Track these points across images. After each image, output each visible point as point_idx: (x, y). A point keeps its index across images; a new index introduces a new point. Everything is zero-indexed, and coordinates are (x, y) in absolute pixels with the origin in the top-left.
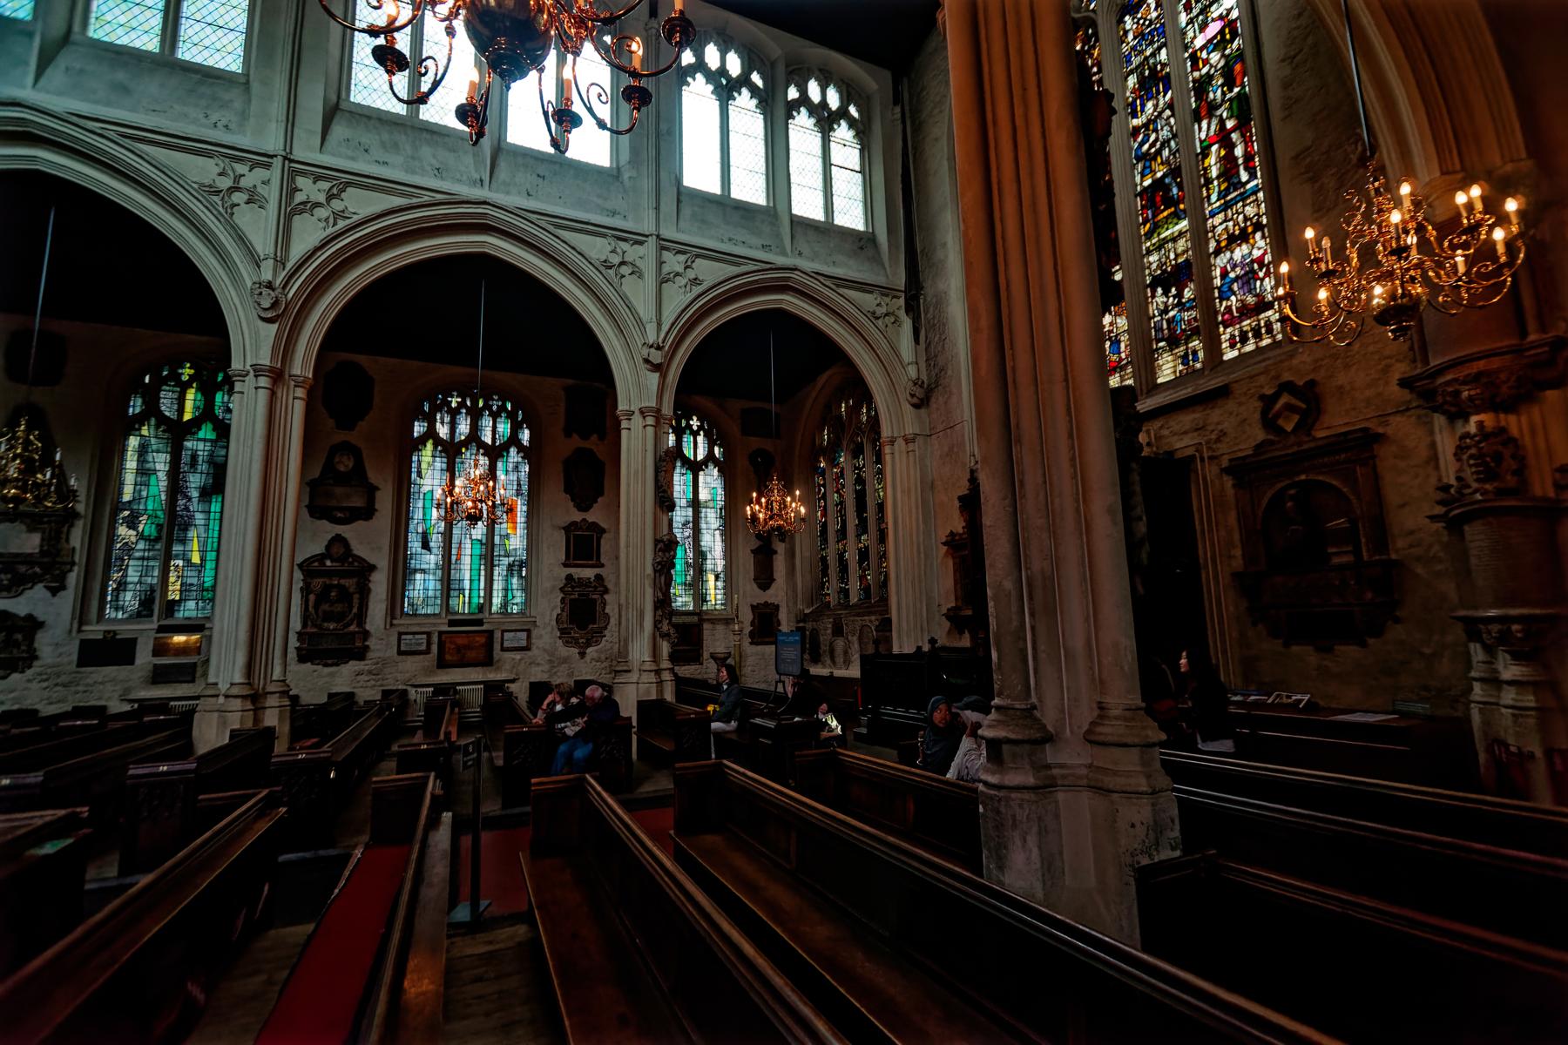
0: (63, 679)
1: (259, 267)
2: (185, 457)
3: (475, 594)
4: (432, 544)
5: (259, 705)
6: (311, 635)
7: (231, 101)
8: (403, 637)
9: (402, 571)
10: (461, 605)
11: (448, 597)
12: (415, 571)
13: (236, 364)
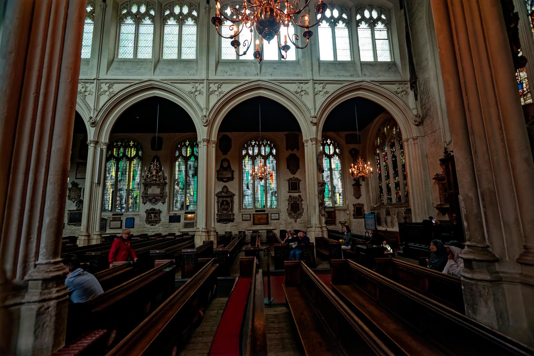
0: (166, 226)
1: (202, 111)
2: (188, 166)
3: (262, 202)
4: (249, 187)
5: (209, 234)
6: (220, 215)
8: (243, 215)
9: (242, 196)
10: (259, 206)
11: (255, 203)
12: (245, 195)
13: (199, 140)
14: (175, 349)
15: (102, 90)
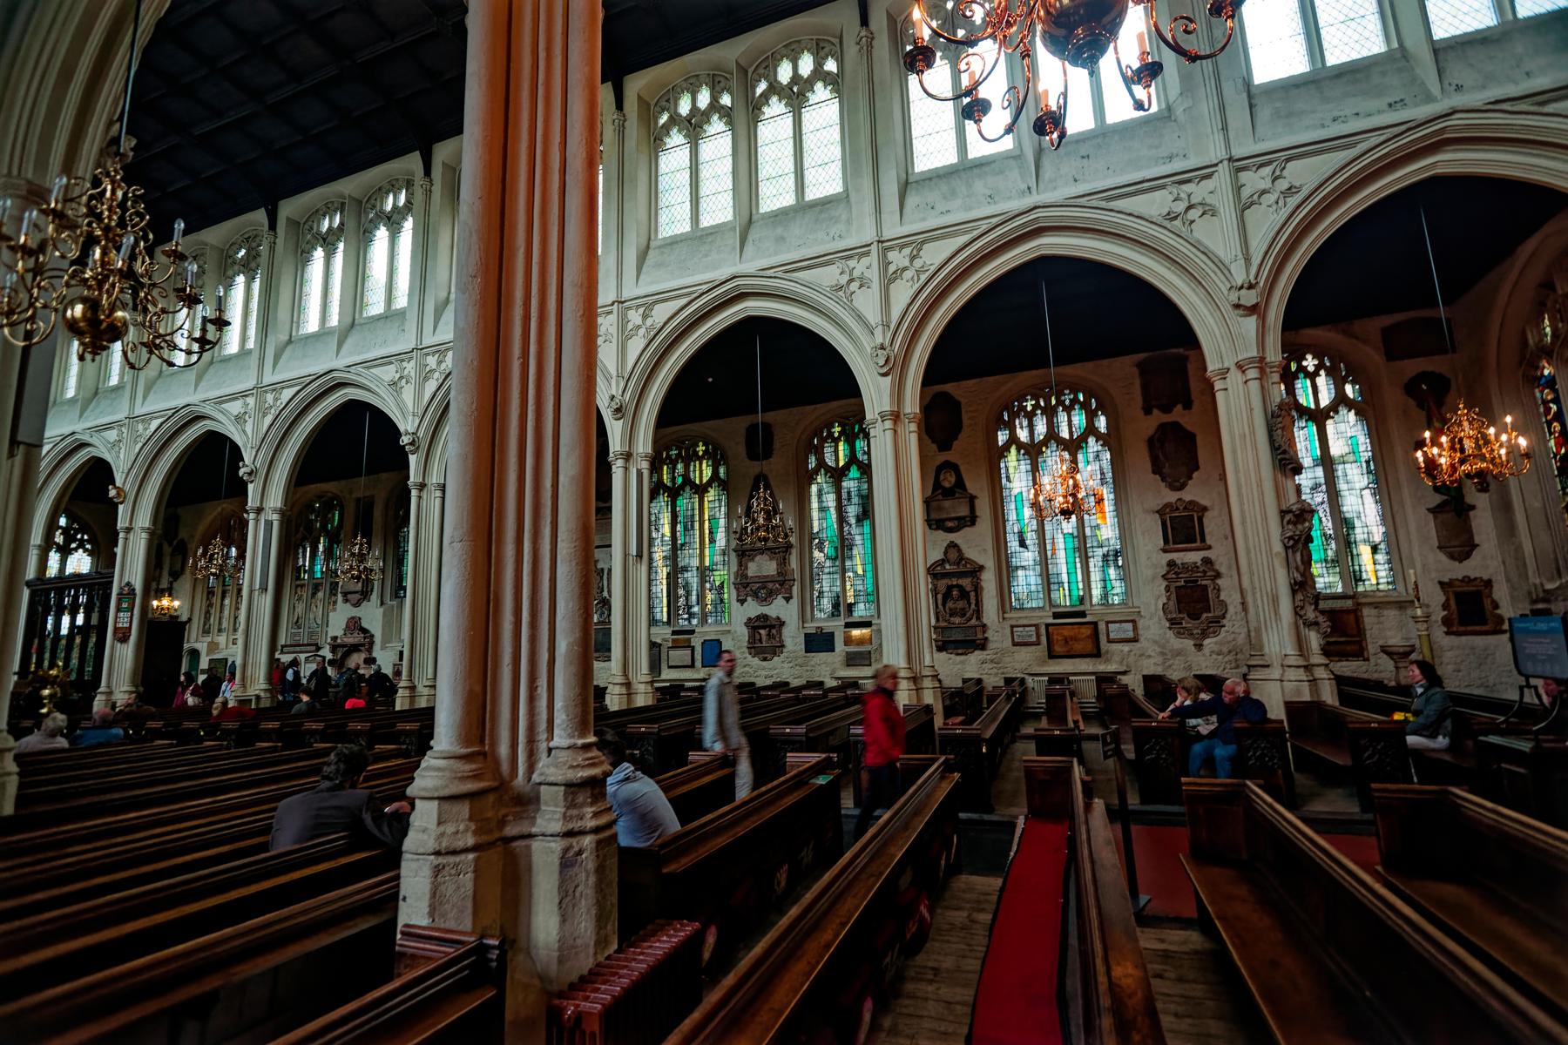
1: (872, 333)
2: (844, 496)
3: (1074, 586)
4: (1028, 542)
5: (919, 686)
6: (943, 628)
7: (840, 215)
8: (1015, 629)
9: (1006, 571)
10: (1063, 598)
11: (1049, 590)
12: (1017, 568)
13: (869, 416)
14: (868, 1005)
15: (630, 326)
